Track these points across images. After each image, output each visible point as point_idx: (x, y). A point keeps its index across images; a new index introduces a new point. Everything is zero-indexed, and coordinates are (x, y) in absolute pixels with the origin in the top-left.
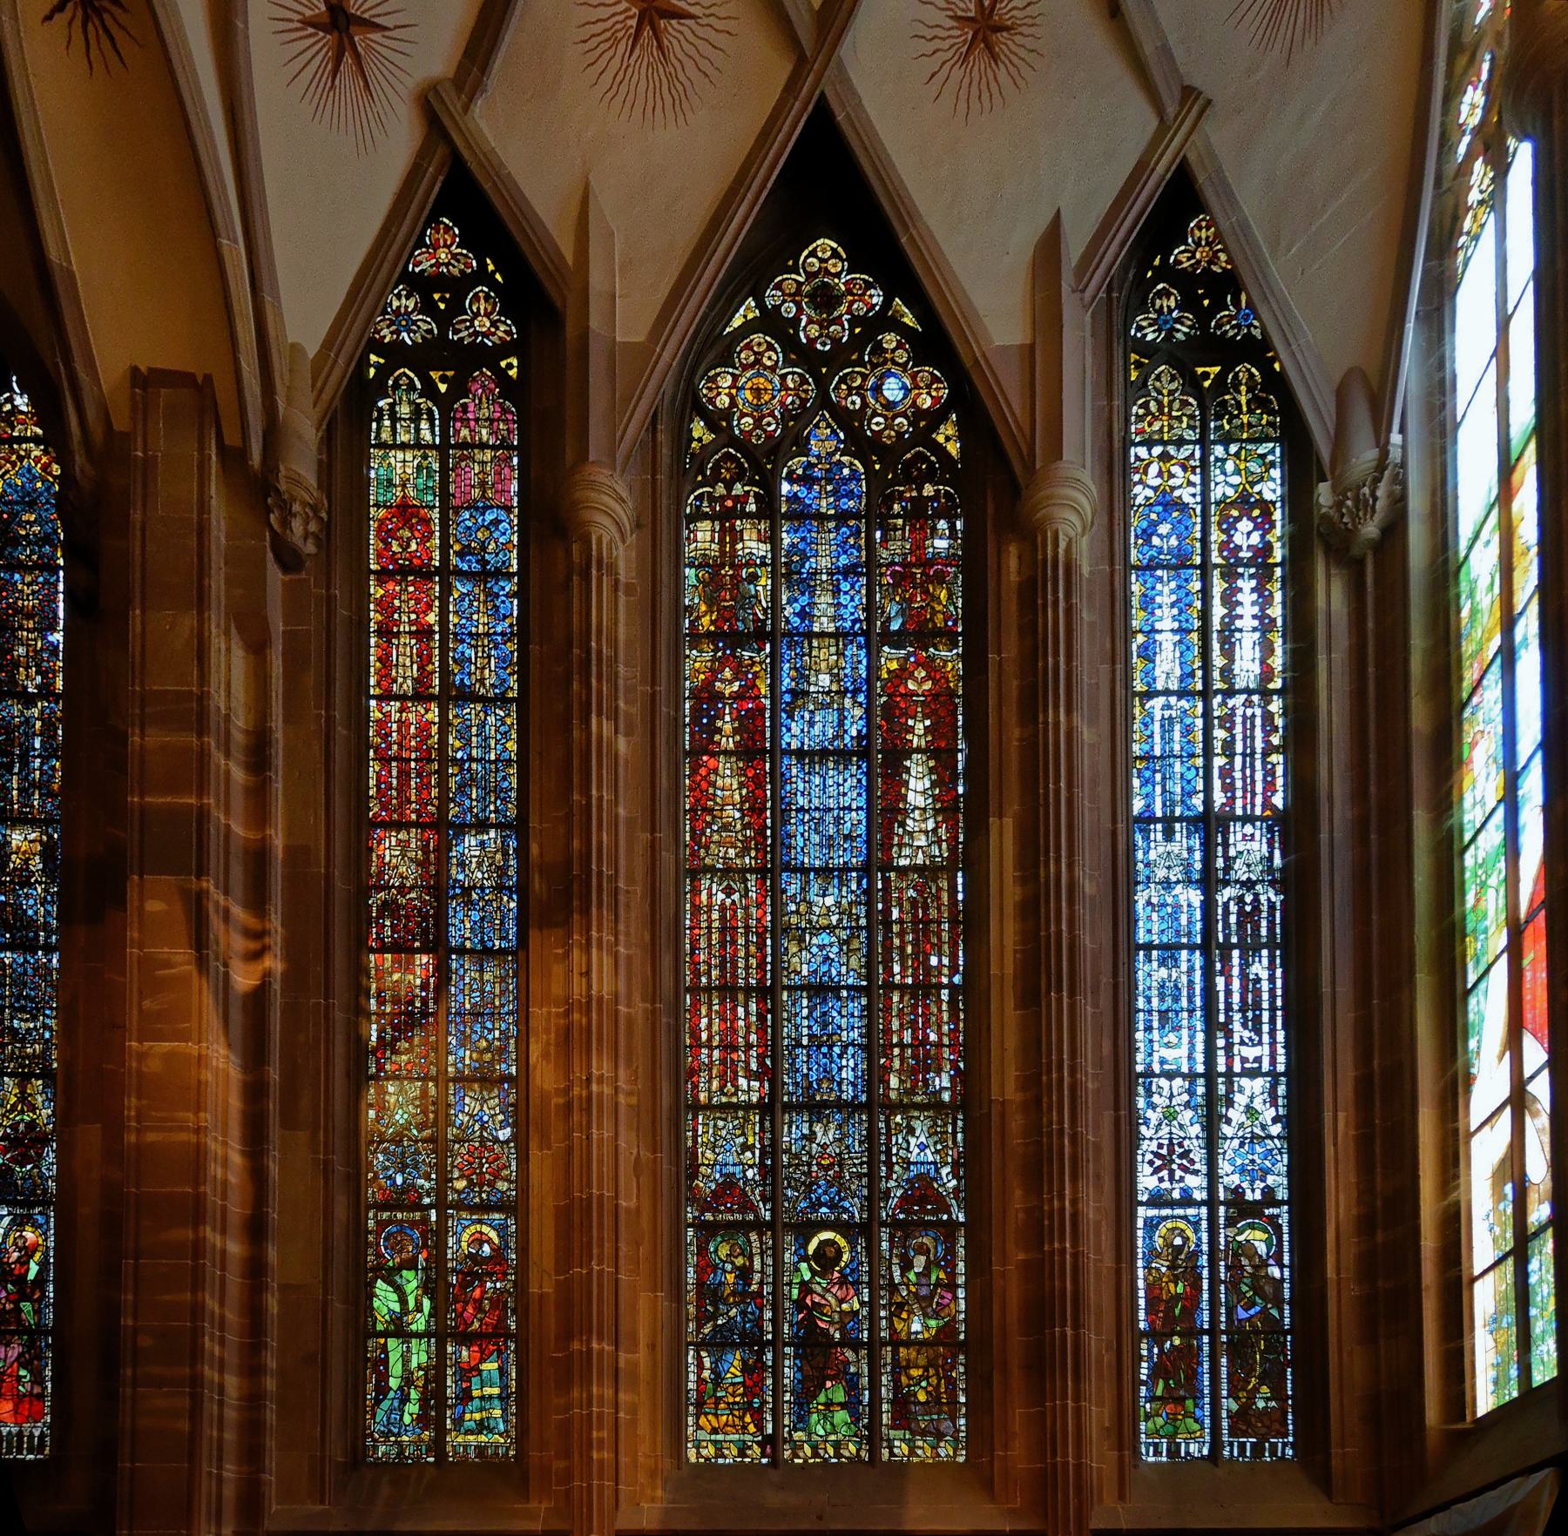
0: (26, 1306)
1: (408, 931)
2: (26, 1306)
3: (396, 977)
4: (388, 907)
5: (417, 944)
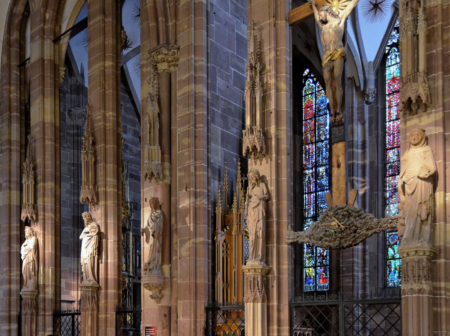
0: (324, 261)
1: (395, 171)
2: (324, 261)
3: (392, 181)
4: (391, 167)
5: (397, 174)
